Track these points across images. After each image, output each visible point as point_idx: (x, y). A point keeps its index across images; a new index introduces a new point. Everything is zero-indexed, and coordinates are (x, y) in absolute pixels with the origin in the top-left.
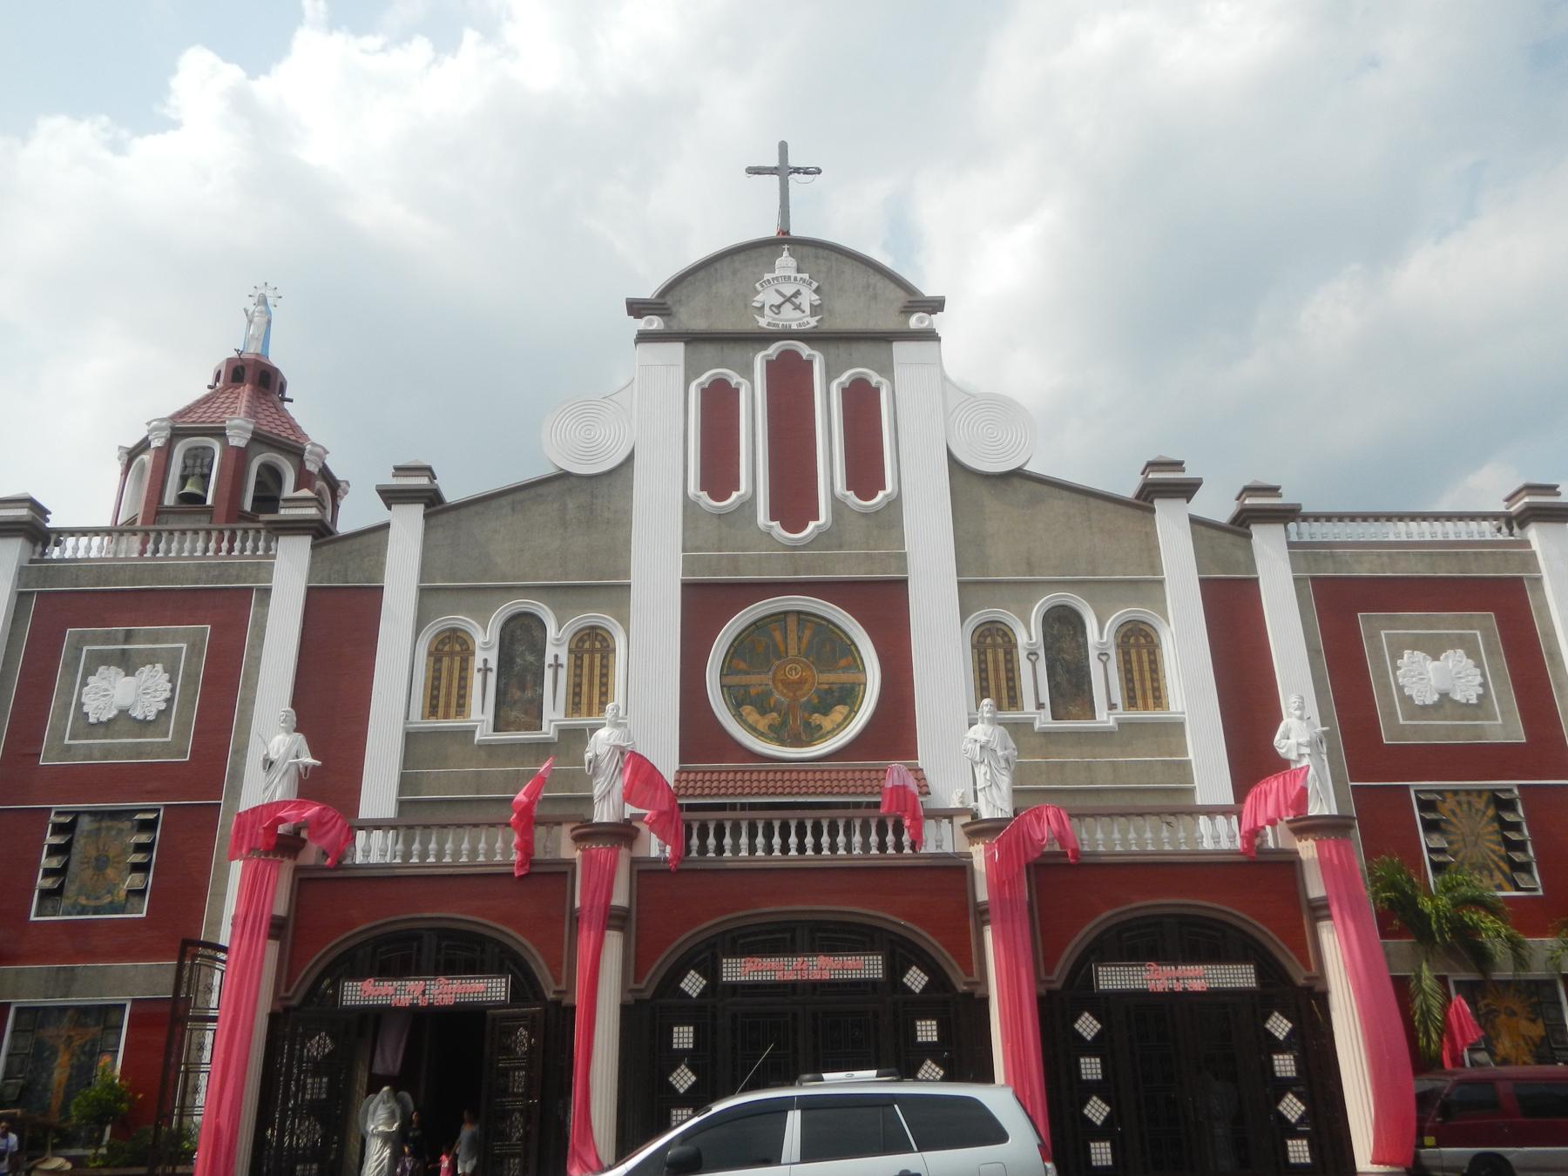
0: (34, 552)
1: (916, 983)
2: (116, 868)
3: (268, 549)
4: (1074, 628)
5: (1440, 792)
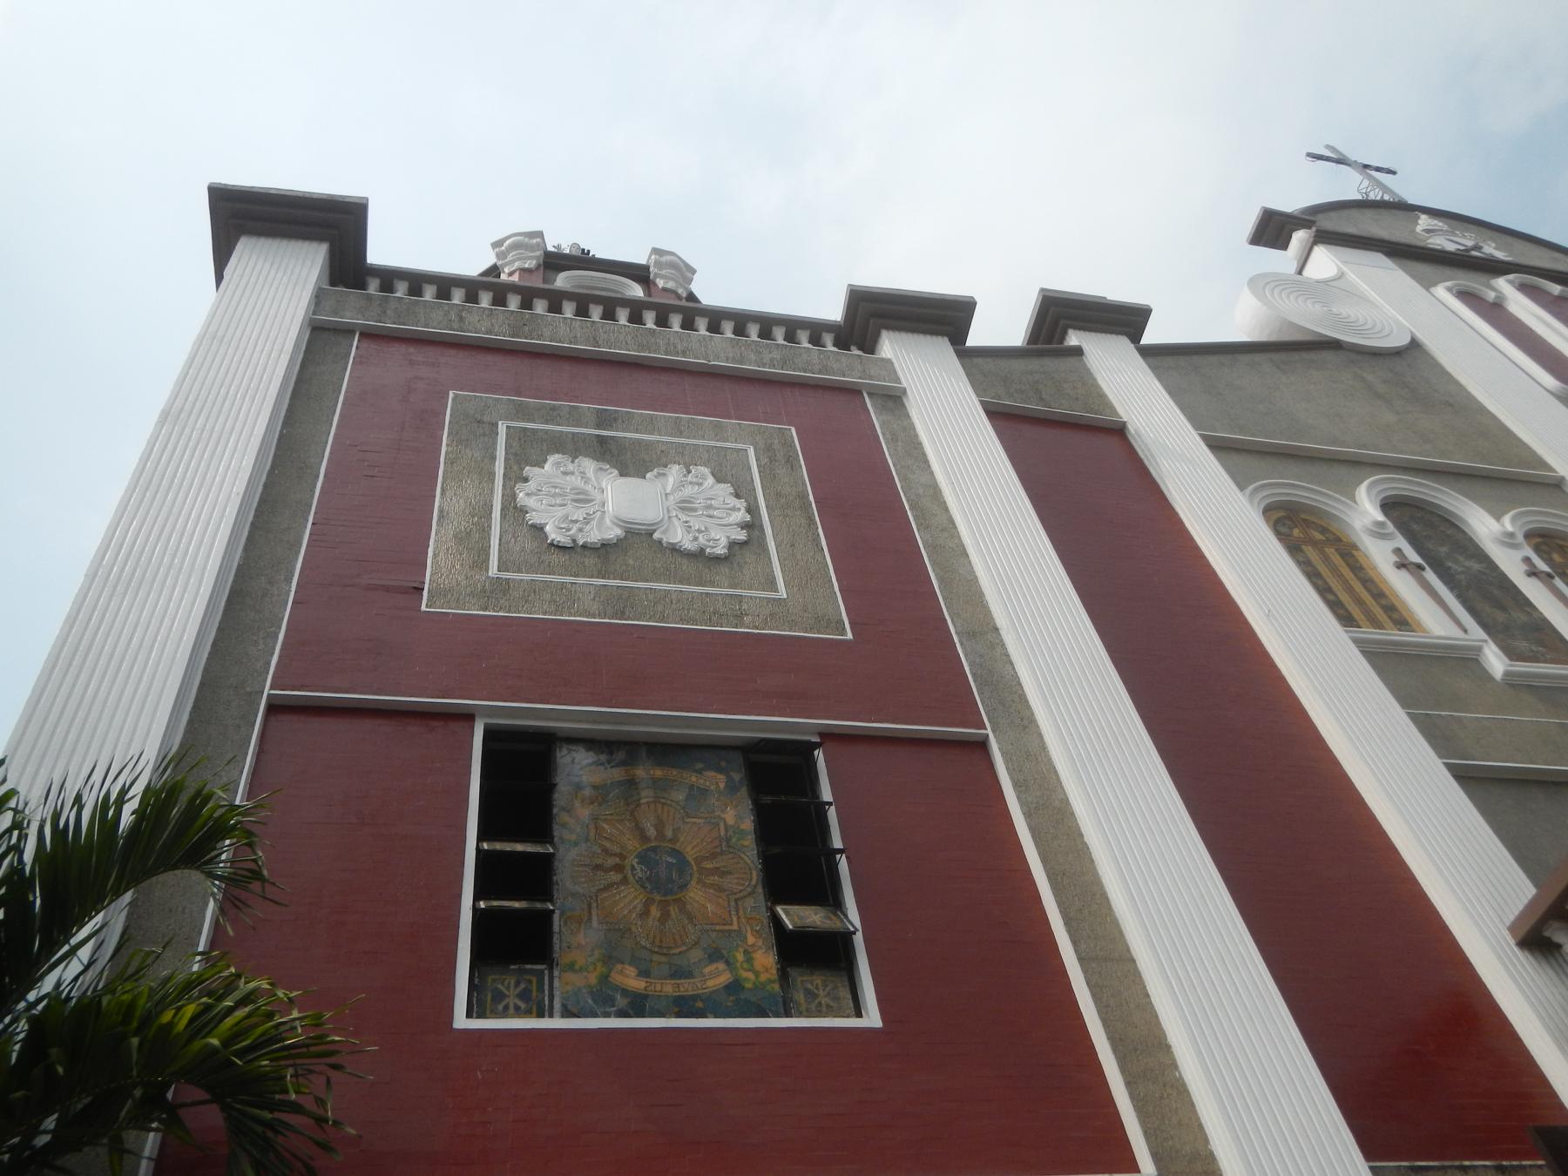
2: (720, 889)
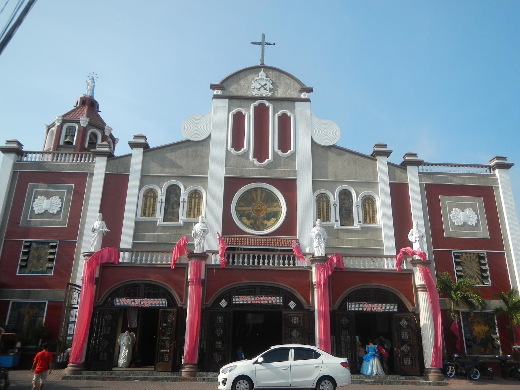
0: (18, 158)
1: (292, 306)
2: (43, 260)
3: (93, 160)
4: (349, 197)
5: (461, 253)
